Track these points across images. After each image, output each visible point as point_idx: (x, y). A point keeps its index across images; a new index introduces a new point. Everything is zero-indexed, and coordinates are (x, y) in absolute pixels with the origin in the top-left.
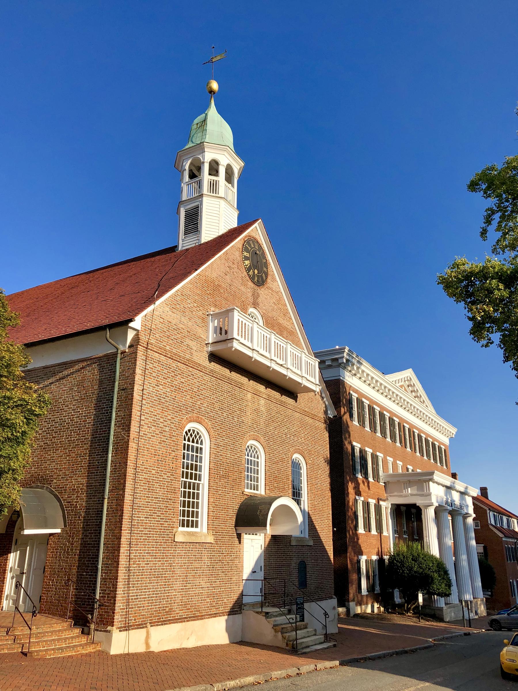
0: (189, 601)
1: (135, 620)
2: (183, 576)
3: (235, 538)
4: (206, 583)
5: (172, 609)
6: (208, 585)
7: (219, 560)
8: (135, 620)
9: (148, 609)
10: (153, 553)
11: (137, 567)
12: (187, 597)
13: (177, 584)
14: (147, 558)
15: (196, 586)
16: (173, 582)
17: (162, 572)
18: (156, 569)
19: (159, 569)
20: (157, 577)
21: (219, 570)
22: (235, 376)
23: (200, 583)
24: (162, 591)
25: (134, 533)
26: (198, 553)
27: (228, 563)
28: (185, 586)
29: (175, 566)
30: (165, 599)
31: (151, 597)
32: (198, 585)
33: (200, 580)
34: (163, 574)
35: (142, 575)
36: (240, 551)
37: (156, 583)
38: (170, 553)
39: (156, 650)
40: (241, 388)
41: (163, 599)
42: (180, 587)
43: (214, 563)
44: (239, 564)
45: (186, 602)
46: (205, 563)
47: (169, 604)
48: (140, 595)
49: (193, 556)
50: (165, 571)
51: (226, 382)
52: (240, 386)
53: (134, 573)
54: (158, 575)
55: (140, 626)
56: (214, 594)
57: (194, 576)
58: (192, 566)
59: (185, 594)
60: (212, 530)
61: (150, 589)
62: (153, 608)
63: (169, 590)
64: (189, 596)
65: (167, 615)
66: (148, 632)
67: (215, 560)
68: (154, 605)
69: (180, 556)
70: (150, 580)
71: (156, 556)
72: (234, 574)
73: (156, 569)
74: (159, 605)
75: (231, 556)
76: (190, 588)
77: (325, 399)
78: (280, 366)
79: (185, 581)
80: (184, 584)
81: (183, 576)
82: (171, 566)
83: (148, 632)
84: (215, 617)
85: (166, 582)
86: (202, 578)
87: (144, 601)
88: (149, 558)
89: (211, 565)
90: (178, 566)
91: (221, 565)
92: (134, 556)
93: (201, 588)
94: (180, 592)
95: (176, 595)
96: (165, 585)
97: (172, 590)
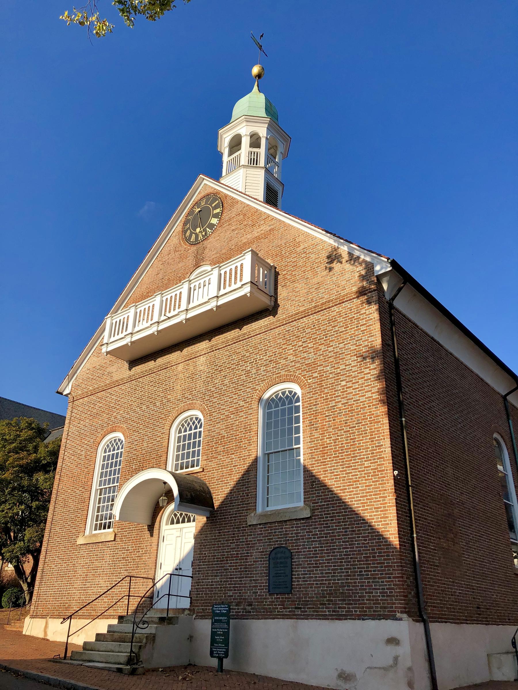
0: (86, 600)
1: (43, 611)
2: (84, 575)
3: (145, 531)
4: (105, 582)
5: (71, 605)
6: (108, 584)
7: (123, 558)
8: (43, 611)
9: (52, 603)
10: (61, 556)
11: (49, 569)
12: (85, 595)
13: (77, 583)
14: (56, 561)
15: (94, 584)
16: (74, 581)
17: (67, 572)
18: (62, 570)
19: (64, 570)
20: (62, 577)
21: (122, 568)
22: (161, 361)
23: (99, 582)
24: (65, 588)
25: (50, 543)
26: (100, 553)
27: (134, 559)
28: (84, 585)
29: (78, 566)
30: (66, 596)
31: (56, 594)
32: (97, 584)
33: (100, 579)
34: (67, 574)
35: (52, 575)
36: (151, 545)
37: (61, 581)
38: (75, 555)
39: (51, 640)
40: (168, 368)
41: (64, 596)
42: (79, 585)
43: (116, 561)
44: (149, 561)
45: (84, 600)
46: (106, 562)
47: (69, 600)
48: (48, 592)
49: (95, 555)
50: (69, 572)
51: (148, 375)
53: (46, 573)
54: (63, 575)
55: (43, 617)
56: (113, 594)
57: (94, 575)
58: (92, 565)
59: (84, 593)
60: (118, 527)
61: (56, 586)
62: (56, 603)
63: (70, 588)
64: (87, 595)
65: (67, 610)
66: (47, 623)
67: (118, 558)
68: (57, 601)
69: (83, 556)
70: (56, 580)
71: (63, 558)
72: (140, 572)
73: (62, 570)
74: (61, 601)
75: (139, 552)
76: (89, 587)
77: (362, 257)
78: (169, 320)
79: (85, 580)
80: (83, 582)
81: (84, 575)
82: (74, 567)
83: (47, 623)
84: (108, 618)
85: (69, 581)
86: (102, 577)
87: (51, 596)
88: (58, 561)
89: (113, 564)
90: (80, 566)
91: (124, 563)
92: (48, 560)
93: (100, 587)
94: (79, 590)
95: (75, 593)
96: (68, 583)
97: (73, 588)
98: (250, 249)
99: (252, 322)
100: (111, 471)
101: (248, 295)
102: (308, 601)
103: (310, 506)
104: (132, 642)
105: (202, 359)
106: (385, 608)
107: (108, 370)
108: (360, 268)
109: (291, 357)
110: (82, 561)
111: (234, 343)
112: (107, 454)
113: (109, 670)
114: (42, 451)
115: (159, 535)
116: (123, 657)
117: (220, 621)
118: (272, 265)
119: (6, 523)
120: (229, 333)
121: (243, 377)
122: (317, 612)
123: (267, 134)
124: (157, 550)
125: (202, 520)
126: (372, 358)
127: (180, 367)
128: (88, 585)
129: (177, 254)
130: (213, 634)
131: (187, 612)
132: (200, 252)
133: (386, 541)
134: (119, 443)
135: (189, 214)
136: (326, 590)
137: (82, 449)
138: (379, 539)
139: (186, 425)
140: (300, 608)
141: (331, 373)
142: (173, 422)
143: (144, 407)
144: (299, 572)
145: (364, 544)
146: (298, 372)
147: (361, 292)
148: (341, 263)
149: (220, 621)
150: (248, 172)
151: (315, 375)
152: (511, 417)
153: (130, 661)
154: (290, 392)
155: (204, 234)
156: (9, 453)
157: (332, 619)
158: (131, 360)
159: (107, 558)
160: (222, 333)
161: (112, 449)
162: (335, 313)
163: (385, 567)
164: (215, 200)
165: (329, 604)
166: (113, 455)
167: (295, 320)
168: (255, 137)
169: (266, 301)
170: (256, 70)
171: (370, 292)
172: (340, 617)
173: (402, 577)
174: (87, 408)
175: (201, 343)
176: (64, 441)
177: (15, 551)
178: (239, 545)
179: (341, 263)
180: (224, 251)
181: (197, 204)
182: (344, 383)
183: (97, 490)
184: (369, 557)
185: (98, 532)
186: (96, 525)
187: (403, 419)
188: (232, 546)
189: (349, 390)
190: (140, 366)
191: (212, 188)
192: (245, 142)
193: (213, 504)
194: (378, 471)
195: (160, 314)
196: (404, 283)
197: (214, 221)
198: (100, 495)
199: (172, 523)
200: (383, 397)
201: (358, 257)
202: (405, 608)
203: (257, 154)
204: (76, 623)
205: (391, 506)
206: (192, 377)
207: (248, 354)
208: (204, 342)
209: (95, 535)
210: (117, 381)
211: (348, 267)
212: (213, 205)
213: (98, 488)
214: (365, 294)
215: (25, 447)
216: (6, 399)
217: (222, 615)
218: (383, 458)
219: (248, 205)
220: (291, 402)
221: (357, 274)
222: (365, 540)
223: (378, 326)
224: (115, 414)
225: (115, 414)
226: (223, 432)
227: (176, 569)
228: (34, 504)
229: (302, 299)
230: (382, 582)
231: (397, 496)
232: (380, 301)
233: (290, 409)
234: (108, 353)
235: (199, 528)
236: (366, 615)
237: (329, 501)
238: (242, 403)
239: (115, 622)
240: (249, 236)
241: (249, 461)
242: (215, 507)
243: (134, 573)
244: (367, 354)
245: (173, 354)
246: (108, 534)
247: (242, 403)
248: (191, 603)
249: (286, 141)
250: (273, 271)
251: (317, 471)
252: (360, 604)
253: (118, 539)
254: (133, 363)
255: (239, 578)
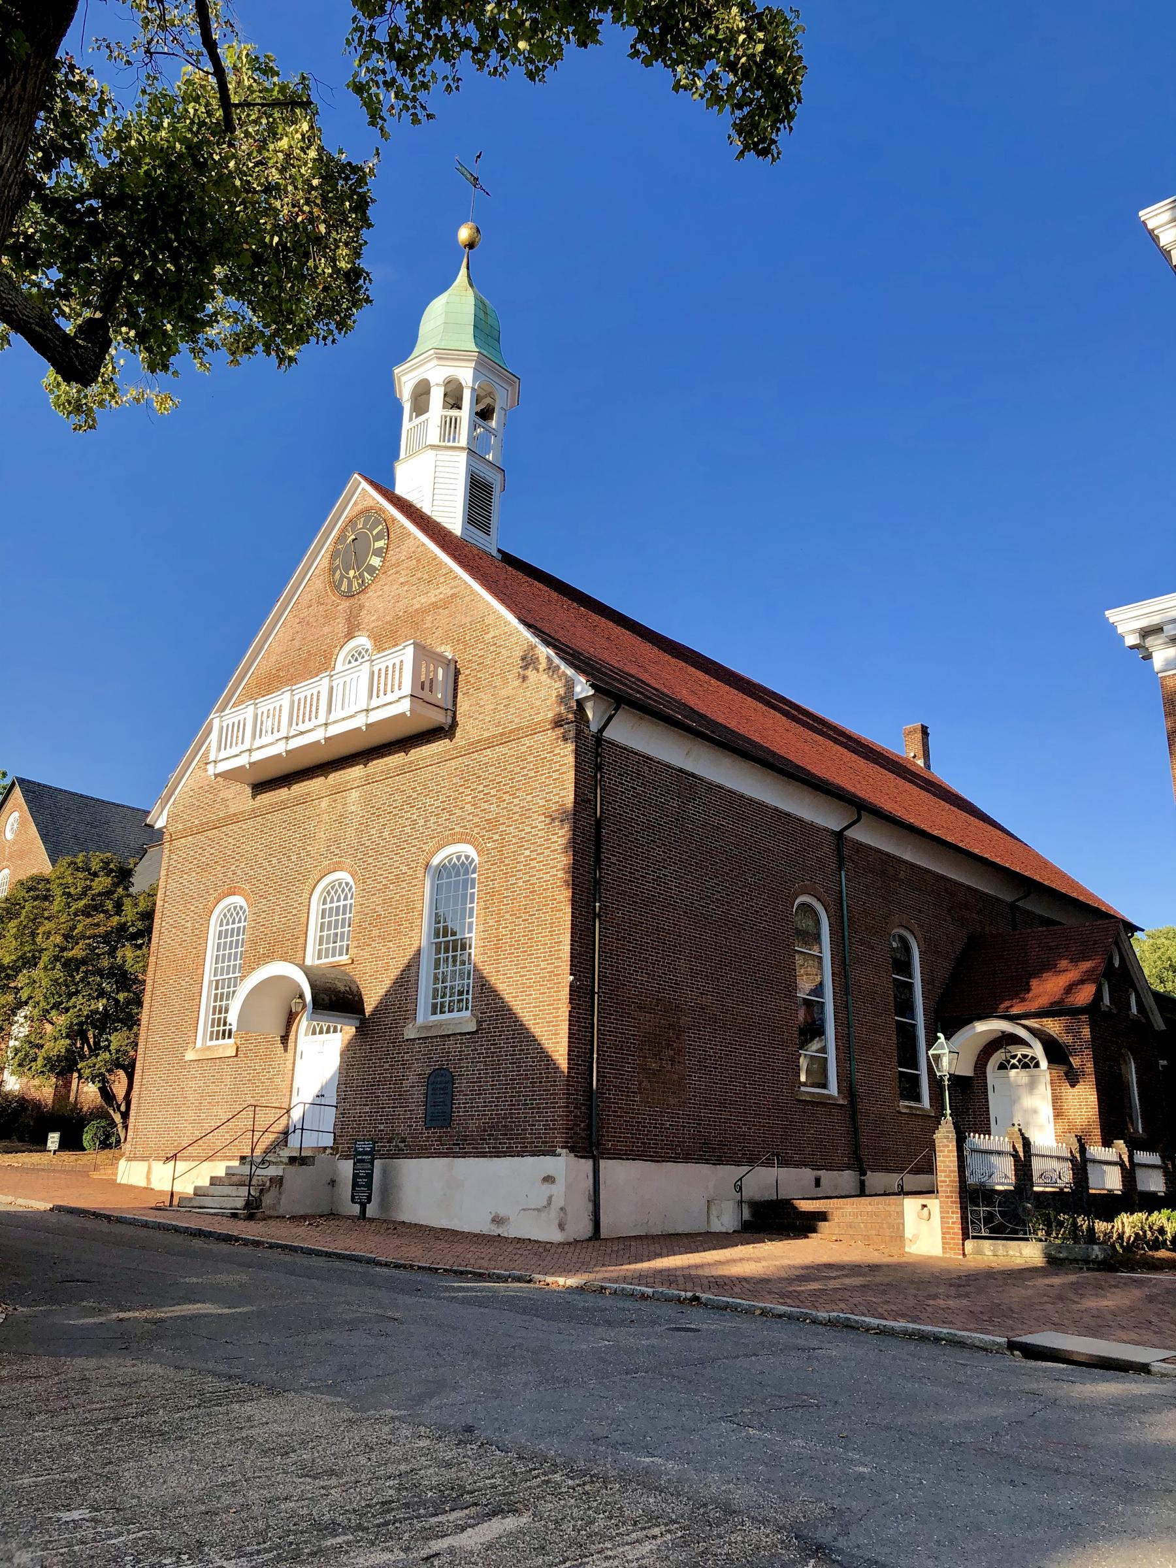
22: (299, 789)
39: (157, 1189)
52: (302, 801)
55: (143, 1159)
98: (412, 641)
99: (422, 745)
100: (230, 954)
101: (408, 714)
102: (468, 1136)
103: (477, 1017)
104: (250, 1185)
105: (354, 795)
106: (546, 1142)
107: (221, 795)
108: (558, 685)
109: (468, 807)
110: (192, 1084)
111: (398, 775)
112: (224, 928)
113: (223, 1215)
114: (130, 913)
115: (295, 1049)
116: (240, 1203)
117: (362, 1161)
118: (450, 657)
119: (80, 1024)
120: (391, 757)
121: (408, 829)
122: (477, 1148)
123: (474, 381)
124: (293, 1070)
125: (350, 1030)
126: (561, 821)
127: (325, 803)
128: (203, 1116)
129: (321, 608)
130: (355, 1176)
131: (328, 1151)
132: (355, 612)
133: (555, 1064)
134: (241, 913)
135: (341, 538)
136: (488, 1123)
137: (188, 918)
138: (548, 1061)
139: (333, 893)
140: (459, 1144)
141: (514, 837)
142: (313, 890)
143: (274, 861)
144: (460, 1099)
145: (531, 1066)
146: (476, 830)
147: (558, 723)
148: (538, 670)
149: (362, 1161)
150: (439, 457)
151: (496, 837)
152: (849, 865)
153: (248, 1205)
154: (467, 857)
155: (360, 581)
156: (76, 915)
157: (491, 1157)
158: (257, 782)
159: (228, 1081)
160: (383, 756)
161: (231, 921)
162: (524, 749)
163: (551, 1094)
164: (377, 523)
165: (490, 1139)
166: (233, 929)
167: (477, 751)
168: (452, 387)
169: (440, 718)
170: (464, 233)
171: (568, 723)
172: (498, 1154)
173: (567, 1107)
174: (192, 853)
175: (354, 768)
176: (162, 884)
177: (97, 1067)
178: (393, 1065)
179: (538, 670)
180: (388, 618)
181: (351, 522)
182: (527, 853)
183: (211, 982)
184: (536, 1082)
185: (214, 1042)
186: (212, 1032)
187: (597, 904)
188: (386, 1066)
189: (533, 863)
190: (267, 795)
191: (374, 499)
192: (437, 397)
193: (364, 1009)
194: (555, 975)
195: (290, 724)
196: (616, 709)
197: (376, 561)
198: (217, 989)
199: (314, 1033)
200: (568, 877)
201: (558, 667)
202: (566, 1142)
203: (456, 419)
204: (181, 1166)
205: (564, 1021)
206: (340, 820)
207: (415, 795)
208: (358, 768)
209: (209, 1048)
210: (235, 815)
211: (544, 677)
212: (374, 533)
213: (213, 978)
214: (562, 726)
215: (102, 905)
216: (61, 790)
217: (366, 1153)
218: (561, 958)
219: (423, 545)
220: (466, 872)
221: (554, 693)
222: (533, 1062)
223: (571, 775)
224: (233, 868)
225: (233, 868)
226: (378, 908)
227: (318, 1096)
228: (121, 997)
229: (488, 719)
230: (546, 1112)
231: (572, 1008)
232: (579, 738)
233: (466, 881)
234: (216, 776)
235: (346, 1042)
236: (526, 1152)
237: (499, 1011)
238: (404, 869)
239: (236, 1163)
240: (423, 599)
241: (410, 953)
242: (367, 1014)
243: (263, 1101)
244: (555, 815)
245: (314, 780)
246: (227, 1047)
247: (404, 869)
248: (334, 1140)
249: (511, 385)
250: (452, 666)
251: (488, 970)
252: (522, 1139)
253: (241, 1054)
254: (260, 787)
255: (393, 1107)
